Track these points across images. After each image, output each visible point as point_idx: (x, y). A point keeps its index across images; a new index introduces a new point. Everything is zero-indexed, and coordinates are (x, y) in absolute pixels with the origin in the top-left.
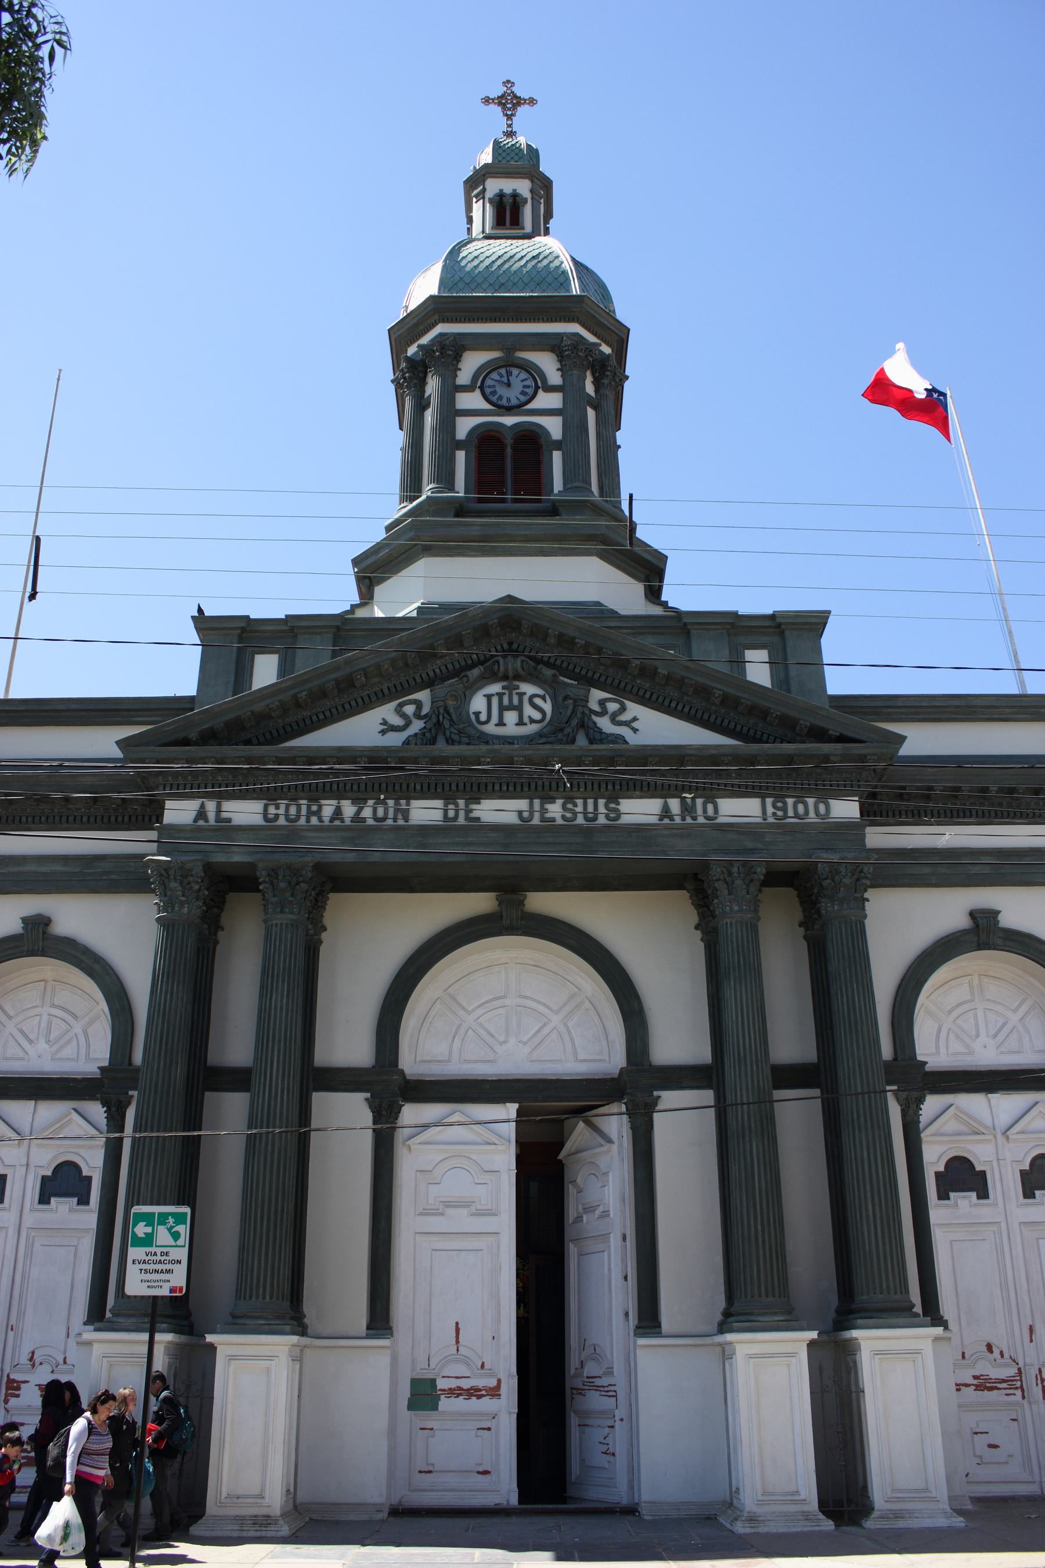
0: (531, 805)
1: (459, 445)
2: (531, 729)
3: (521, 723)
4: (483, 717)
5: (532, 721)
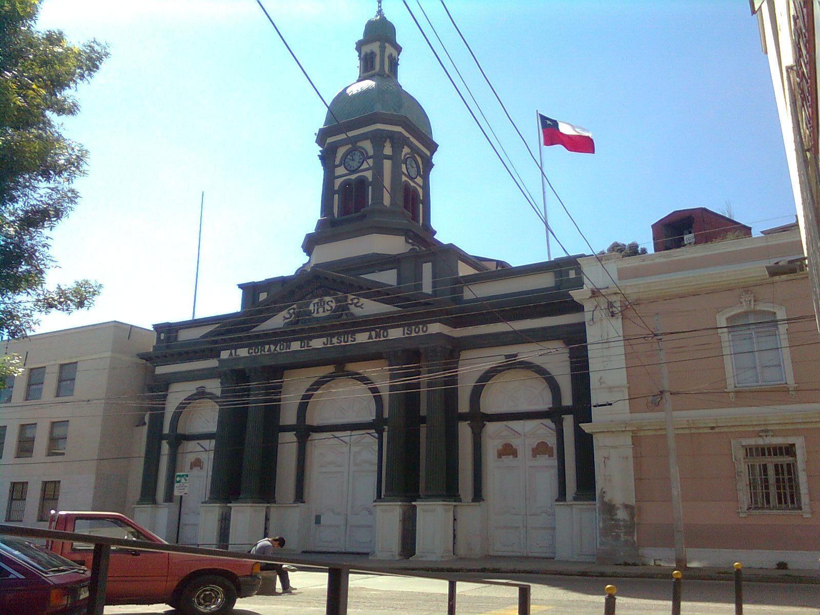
0: (327, 340)
1: (336, 192)
3: (324, 312)
4: (313, 312)
5: (328, 310)
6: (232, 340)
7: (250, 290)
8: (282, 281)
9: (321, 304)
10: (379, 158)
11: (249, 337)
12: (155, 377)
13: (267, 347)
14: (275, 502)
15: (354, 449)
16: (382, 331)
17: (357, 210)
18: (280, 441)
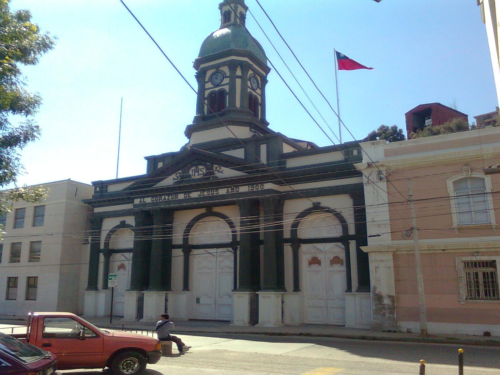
0: (201, 192)
1: (205, 99)
2: (200, 177)
3: (198, 175)
4: (191, 175)
5: (201, 174)
6: (142, 192)
7: (152, 161)
8: (172, 155)
9: (197, 171)
10: (233, 78)
11: (152, 190)
12: (94, 214)
13: (163, 197)
14: (171, 290)
15: (219, 259)
16: (235, 188)
17: (219, 110)
18: (172, 255)
